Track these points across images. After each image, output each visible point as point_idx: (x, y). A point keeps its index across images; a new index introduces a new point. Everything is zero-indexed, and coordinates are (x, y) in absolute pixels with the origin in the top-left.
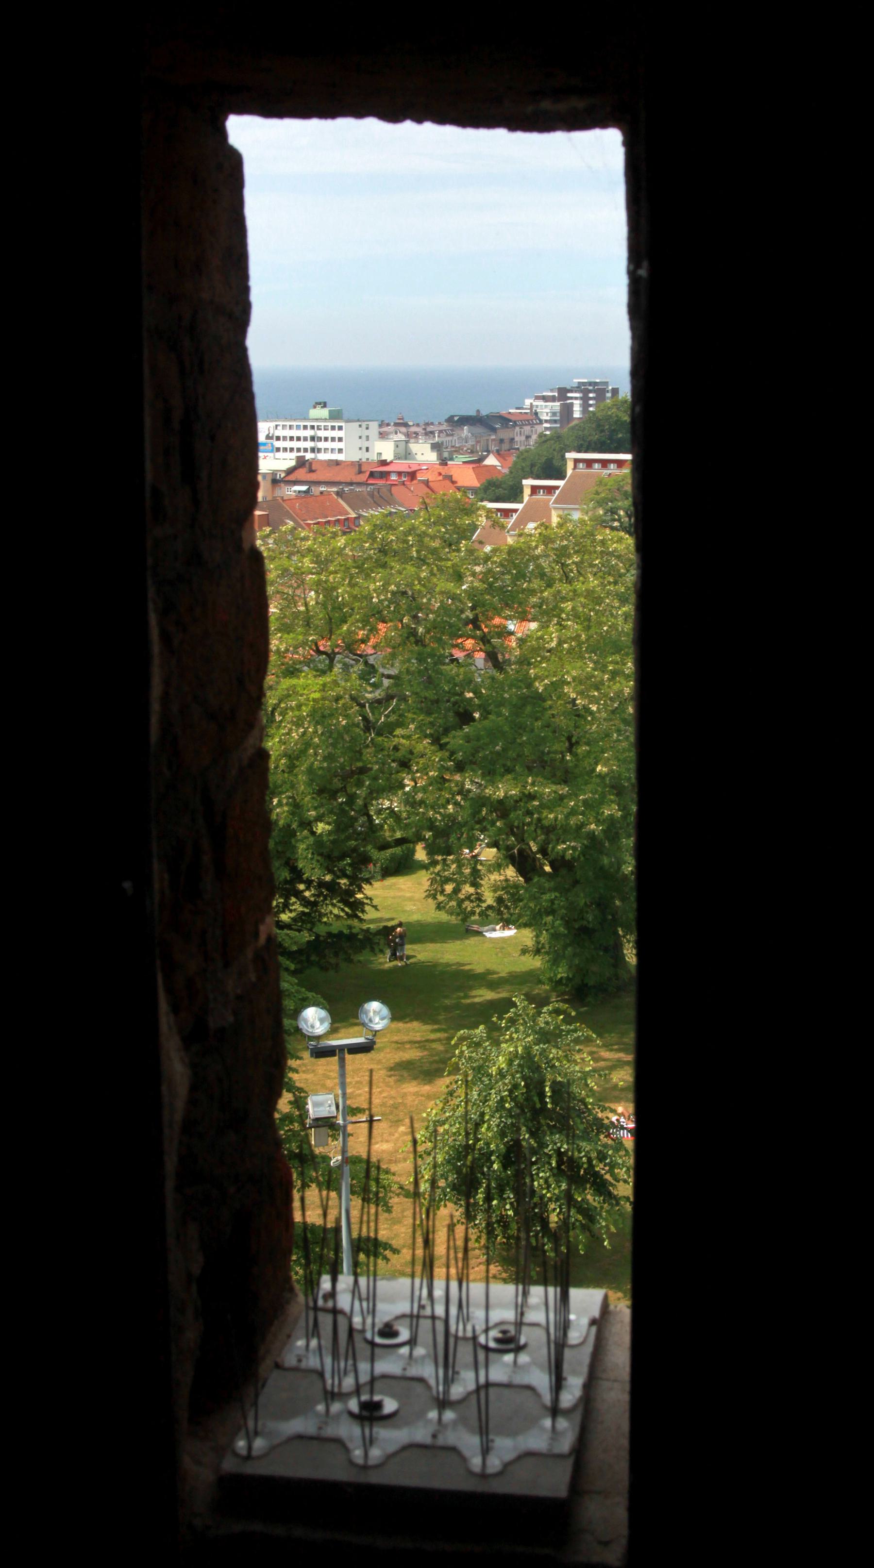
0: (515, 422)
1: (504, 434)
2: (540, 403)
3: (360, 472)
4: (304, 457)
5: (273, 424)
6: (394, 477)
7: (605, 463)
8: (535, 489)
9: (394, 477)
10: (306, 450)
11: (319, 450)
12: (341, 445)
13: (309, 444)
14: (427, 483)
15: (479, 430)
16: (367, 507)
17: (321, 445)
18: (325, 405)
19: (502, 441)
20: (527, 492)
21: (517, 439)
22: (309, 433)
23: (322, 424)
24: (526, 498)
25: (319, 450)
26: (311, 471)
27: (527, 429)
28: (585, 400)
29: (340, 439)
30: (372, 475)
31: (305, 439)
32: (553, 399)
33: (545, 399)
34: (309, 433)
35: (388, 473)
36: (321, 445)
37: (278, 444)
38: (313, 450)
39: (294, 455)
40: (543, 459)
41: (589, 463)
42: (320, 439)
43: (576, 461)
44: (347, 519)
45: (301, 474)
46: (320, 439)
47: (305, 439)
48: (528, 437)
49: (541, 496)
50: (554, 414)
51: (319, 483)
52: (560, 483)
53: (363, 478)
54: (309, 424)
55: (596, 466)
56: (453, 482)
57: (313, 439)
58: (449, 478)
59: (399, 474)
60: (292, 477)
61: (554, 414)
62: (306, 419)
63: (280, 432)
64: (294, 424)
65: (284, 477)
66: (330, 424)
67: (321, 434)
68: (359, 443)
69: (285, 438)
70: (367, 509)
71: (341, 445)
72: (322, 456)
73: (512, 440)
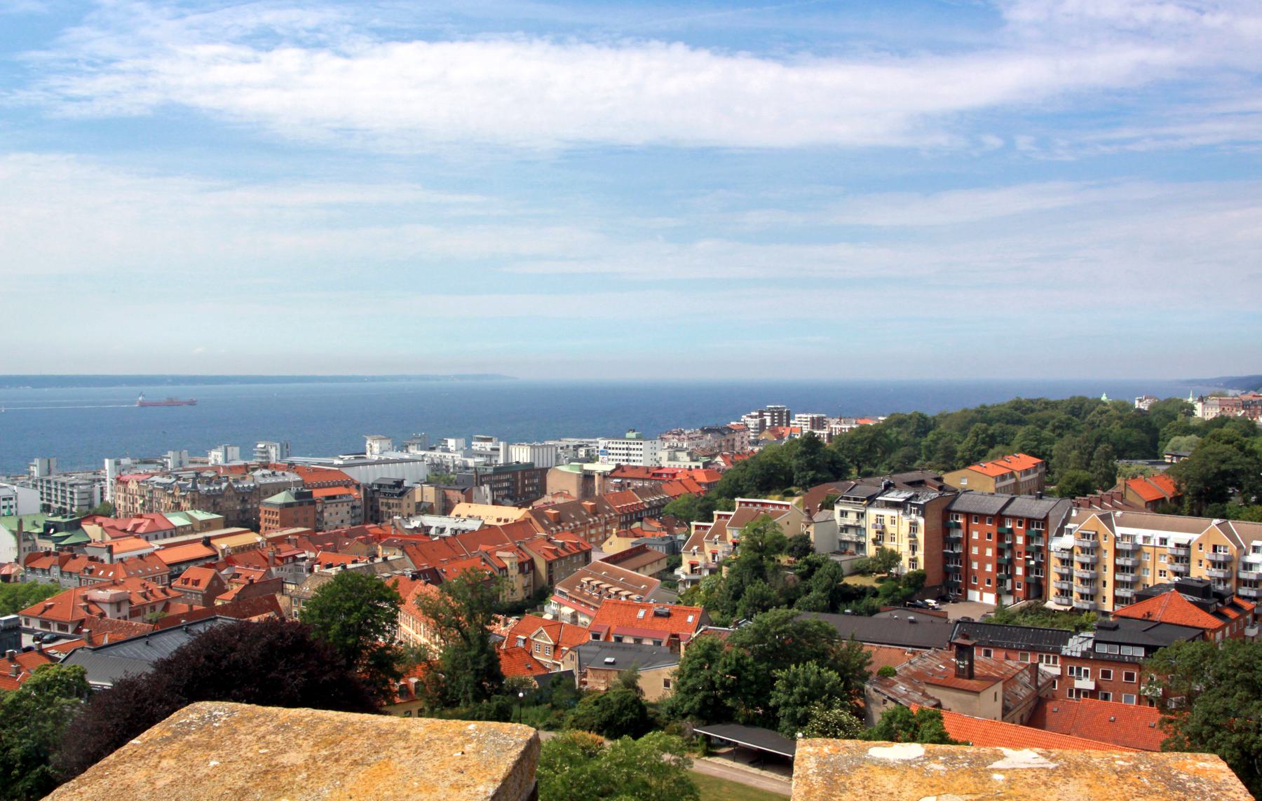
0: (736, 431)
1: (729, 437)
2: (749, 419)
3: (648, 472)
5: (607, 441)
6: (665, 476)
7: (755, 504)
8: (719, 516)
9: (665, 476)
10: (623, 460)
11: (630, 455)
12: (641, 452)
13: (625, 457)
14: (680, 481)
15: (717, 434)
16: (648, 496)
17: (631, 452)
18: (634, 431)
19: (728, 441)
20: (716, 517)
21: (737, 439)
22: (625, 446)
23: (632, 442)
24: (715, 521)
25: (630, 455)
26: (623, 471)
28: (773, 416)
29: (641, 450)
30: (654, 474)
31: (623, 449)
32: (756, 417)
33: (751, 417)
34: (625, 446)
35: (660, 475)
36: (631, 452)
37: (610, 451)
38: (627, 460)
40: (736, 478)
41: (747, 504)
42: (631, 449)
43: (740, 502)
44: (638, 504)
45: (618, 473)
46: (631, 449)
47: (623, 449)
48: (742, 438)
49: (723, 519)
50: (756, 425)
51: (627, 478)
52: (733, 513)
53: (649, 476)
54: (625, 441)
55: (750, 505)
56: (694, 480)
57: (627, 449)
58: (693, 477)
59: (667, 474)
60: (613, 475)
61: (756, 425)
62: (624, 438)
63: (610, 445)
64: (618, 441)
66: (636, 442)
67: (631, 446)
68: (651, 451)
69: (613, 449)
71: (641, 452)
72: (632, 464)
73: (734, 439)
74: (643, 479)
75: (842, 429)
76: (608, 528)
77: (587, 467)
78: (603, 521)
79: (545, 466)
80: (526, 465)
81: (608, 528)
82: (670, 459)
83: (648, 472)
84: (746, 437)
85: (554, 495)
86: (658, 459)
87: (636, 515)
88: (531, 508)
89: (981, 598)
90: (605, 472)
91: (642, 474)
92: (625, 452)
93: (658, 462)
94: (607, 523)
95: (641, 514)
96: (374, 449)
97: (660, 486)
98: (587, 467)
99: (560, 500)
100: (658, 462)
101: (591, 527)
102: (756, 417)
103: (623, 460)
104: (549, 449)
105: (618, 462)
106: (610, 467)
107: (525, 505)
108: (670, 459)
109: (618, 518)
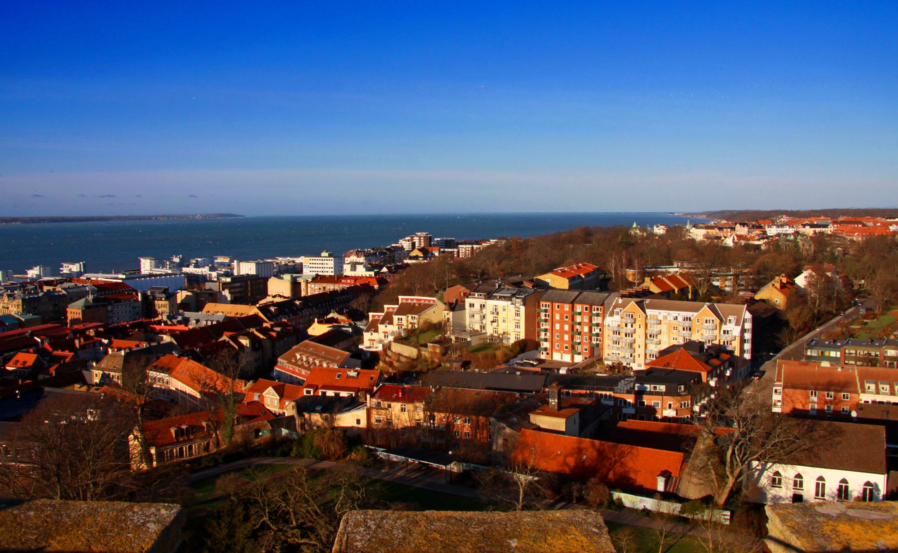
2: (404, 242)
21: (396, 255)
22: (321, 262)
23: (326, 259)
27: (399, 252)
28: (420, 240)
32: (409, 241)
33: (405, 240)
34: (321, 262)
48: (400, 255)
54: (321, 259)
62: (320, 256)
73: (394, 256)
75: (466, 248)
76: (311, 318)
79: (266, 276)
80: (253, 276)
81: (311, 318)
82: (351, 270)
84: (402, 254)
85: (274, 297)
88: (258, 305)
89: (562, 358)
92: (321, 266)
94: (310, 315)
96: (146, 266)
99: (278, 300)
102: (409, 241)
104: (266, 265)
105: (317, 273)
107: (254, 303)
108: (351, 270)
109: (318, 311)
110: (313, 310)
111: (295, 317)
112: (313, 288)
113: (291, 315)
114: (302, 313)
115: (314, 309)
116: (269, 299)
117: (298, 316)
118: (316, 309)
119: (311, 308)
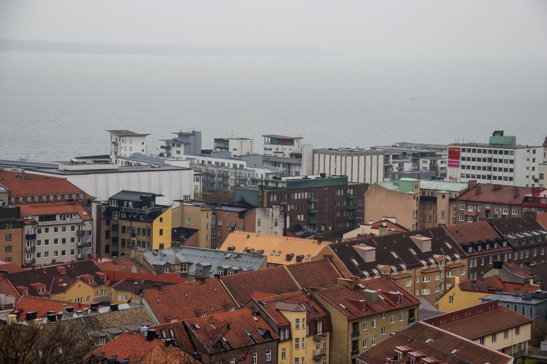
4: (476, 181)
39: (468, 180)
60: (465, 197)
65: (458, 197)
70: (515, 233)
74: (510, 206)
77: (426, 184)
78: (442, 267)
83: (516, 197)
86: (537, 177)
87: (495, 257)
90: (450, 192)
91: (507, 198)
93: (536, 181)
94: (448, 269)
95: (502, 257)
97: (534, 214)
98: (425, 184)
100: (536, 181)
101: (423, 273)
103: (484, 177)
105: (471, 179)
106: (459, 187)
109: (465, 262)
110: (454, 259)
111: (412, 272)
112: (462, 212)
113: (403, 266)
114: (429, 264)
115: (457, 256)
116: (365, 230)
117: (418, 270)
118: (462, 258)
119: (450, 253)
